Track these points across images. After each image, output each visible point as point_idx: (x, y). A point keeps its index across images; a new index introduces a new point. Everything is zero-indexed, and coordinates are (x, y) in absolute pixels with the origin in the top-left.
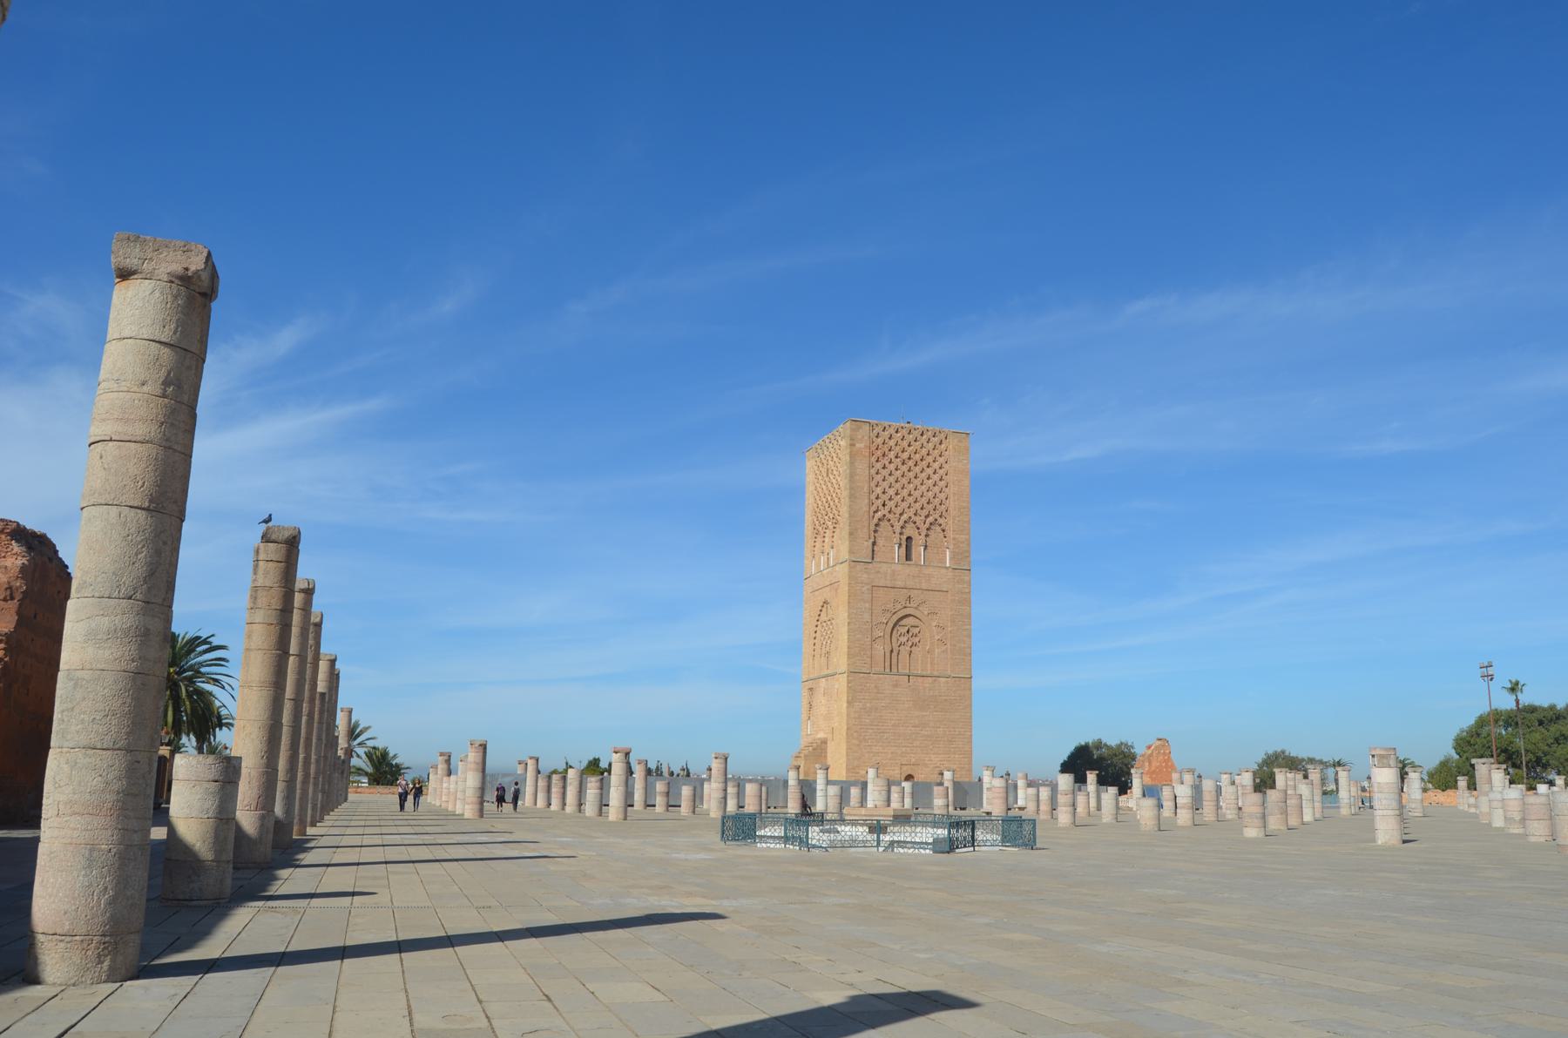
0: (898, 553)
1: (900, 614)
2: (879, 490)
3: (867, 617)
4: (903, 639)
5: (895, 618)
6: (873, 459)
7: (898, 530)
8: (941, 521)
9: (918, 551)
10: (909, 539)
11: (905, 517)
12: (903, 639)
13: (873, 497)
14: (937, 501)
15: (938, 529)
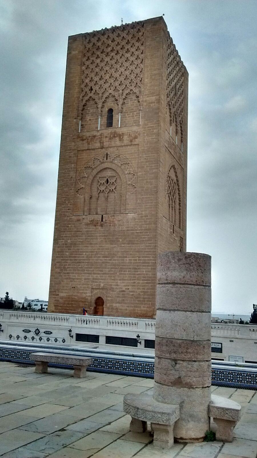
0: (101, 121)
1: (99, 169)
2: (87, 81)
3: (72, 174)
4: (102, 188)
5: (95, 172)
6: (84, 59)
7: (100, 106)
8: (136, 90)
9: (118, 118)
10: (111, 111)
11: (105, 96)
12: (102, 188)
13: (83, 86)
14: (133, 77)
15: (134, 97)
